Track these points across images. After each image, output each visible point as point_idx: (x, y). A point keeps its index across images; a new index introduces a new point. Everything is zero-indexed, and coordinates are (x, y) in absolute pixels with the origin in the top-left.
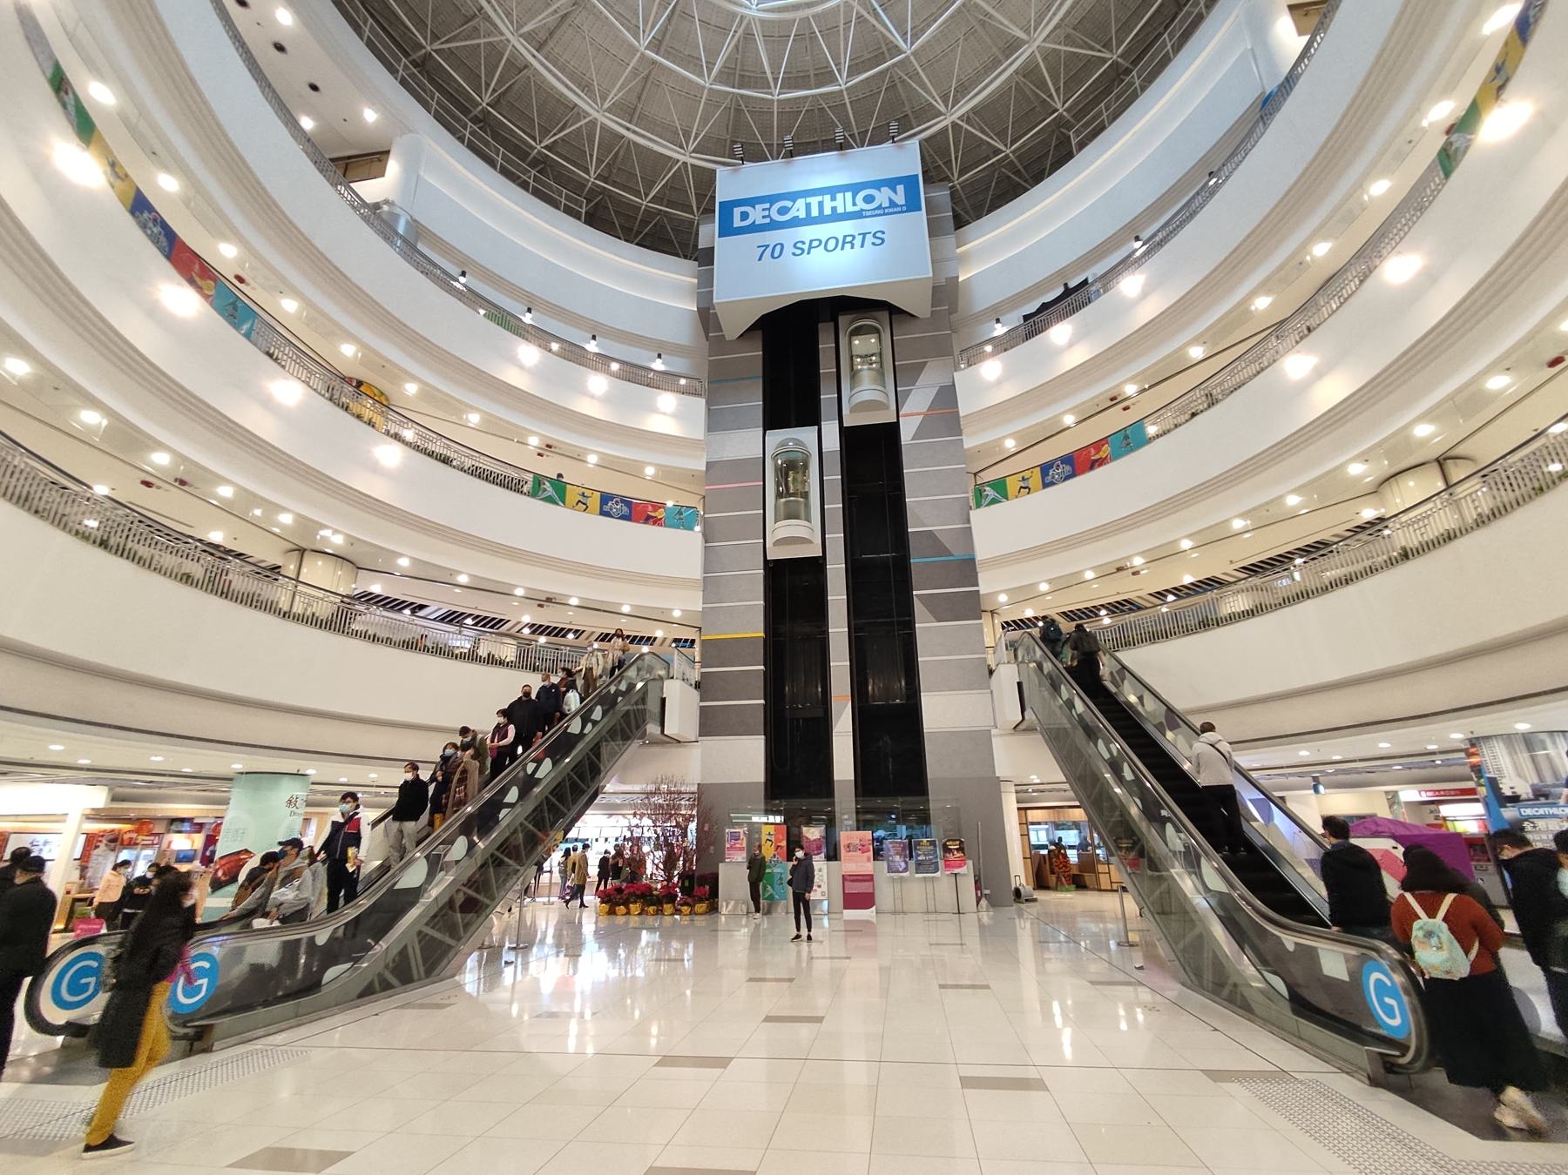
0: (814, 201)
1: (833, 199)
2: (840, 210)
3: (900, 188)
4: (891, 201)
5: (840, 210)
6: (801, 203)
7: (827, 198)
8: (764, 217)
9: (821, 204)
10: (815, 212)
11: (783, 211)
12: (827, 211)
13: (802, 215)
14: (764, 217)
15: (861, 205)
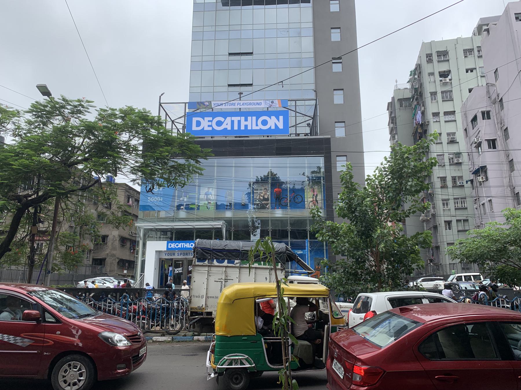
0: (236, 119)
1: (246, 120)
2: (249, 128)
3: (281, 118)
4: (276, 125)
5: (249, 128)
6: (229, 119)
7: (243, 118)
8: (209, 126)
9: (239, 122)
10: (236, 128)
11: (219, 123)
12: (243, 128)
13: (229, 128)
14: (209, 126)
15: (261, 127)
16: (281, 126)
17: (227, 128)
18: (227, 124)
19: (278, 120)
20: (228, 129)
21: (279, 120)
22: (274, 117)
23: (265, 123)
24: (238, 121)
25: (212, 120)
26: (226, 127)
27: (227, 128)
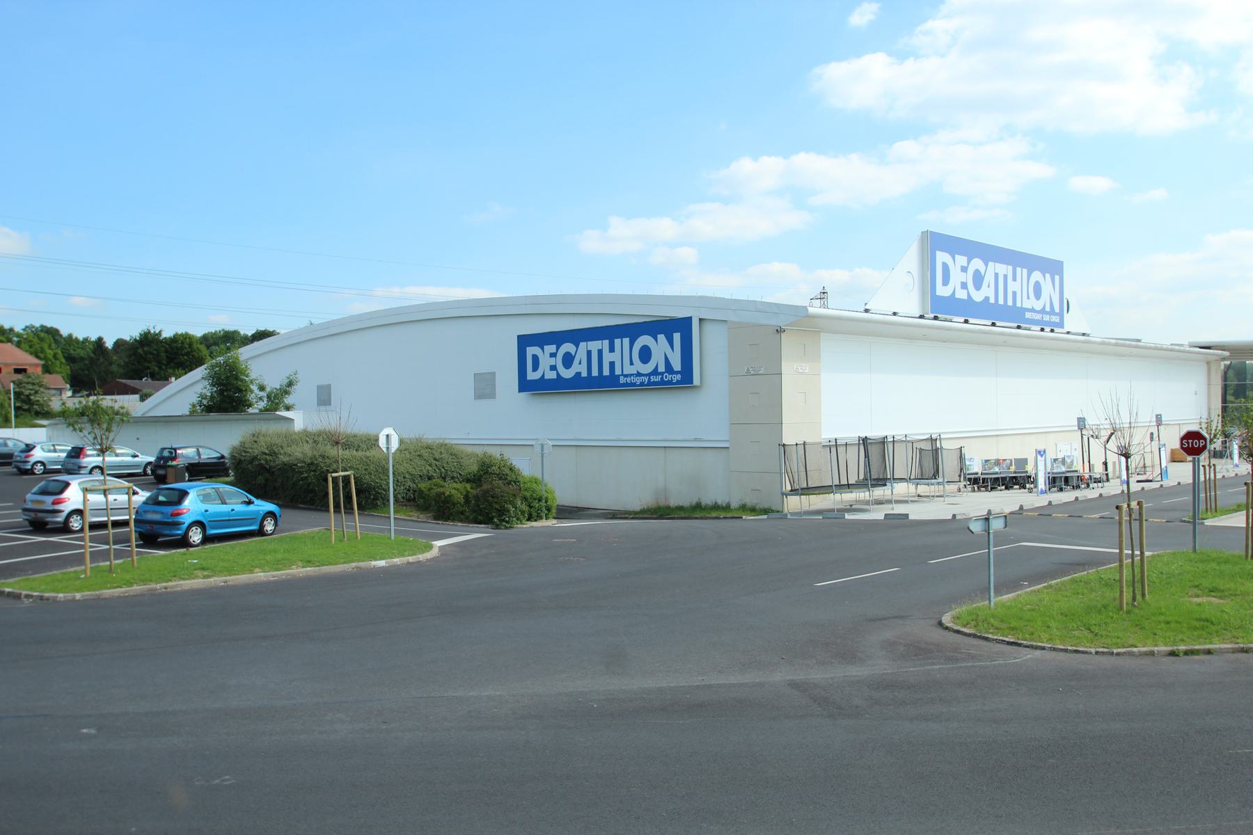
0: (594, 346)
3: (677, 337)
8: (553, 368)
9: (600, 352)
10: (595, 373)
11: (568, 360)
12: (606, 372)
13: (584, 374)
14: (553, 368)
18: (580, 363)
23: (645, 354)
25: (555, 351)
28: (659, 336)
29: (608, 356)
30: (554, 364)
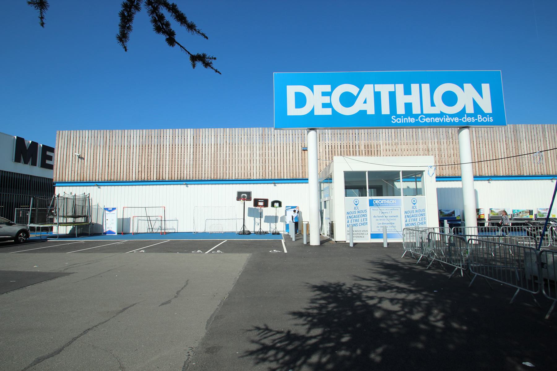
0: (385, 89)
1: (408, 92)
2: (416, 110)
3: (486, 87)
4: (475, 104)
6: (368, 90)
7: (400, 88)
8: (325, 106)
9: (392, 96)
10: (385, 110)
12: (400, 110)
13: (371, 111)
14: (325, 106)
15: (441, 107)
16: (486, 106)
17: (366, 111)
18: (365, 102)
19: (480, 91)
20: (368, 113)
21: (480, 93)
22: (470, 85)
24: (390, 93)
25: (330, 91)
26: (363, 107)
27: (366, 111)
28: (466, 85)
29: (401, 100)
30: (329, 102)
